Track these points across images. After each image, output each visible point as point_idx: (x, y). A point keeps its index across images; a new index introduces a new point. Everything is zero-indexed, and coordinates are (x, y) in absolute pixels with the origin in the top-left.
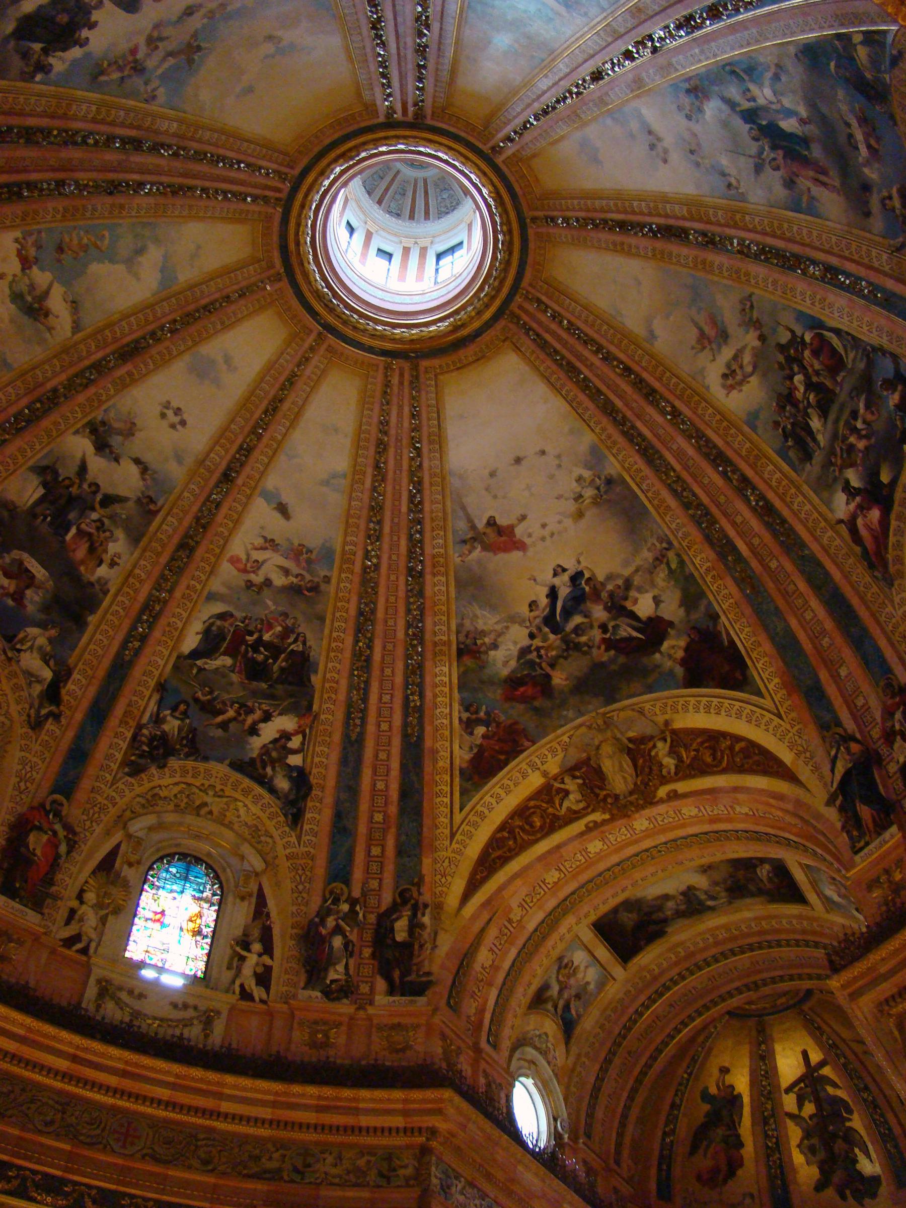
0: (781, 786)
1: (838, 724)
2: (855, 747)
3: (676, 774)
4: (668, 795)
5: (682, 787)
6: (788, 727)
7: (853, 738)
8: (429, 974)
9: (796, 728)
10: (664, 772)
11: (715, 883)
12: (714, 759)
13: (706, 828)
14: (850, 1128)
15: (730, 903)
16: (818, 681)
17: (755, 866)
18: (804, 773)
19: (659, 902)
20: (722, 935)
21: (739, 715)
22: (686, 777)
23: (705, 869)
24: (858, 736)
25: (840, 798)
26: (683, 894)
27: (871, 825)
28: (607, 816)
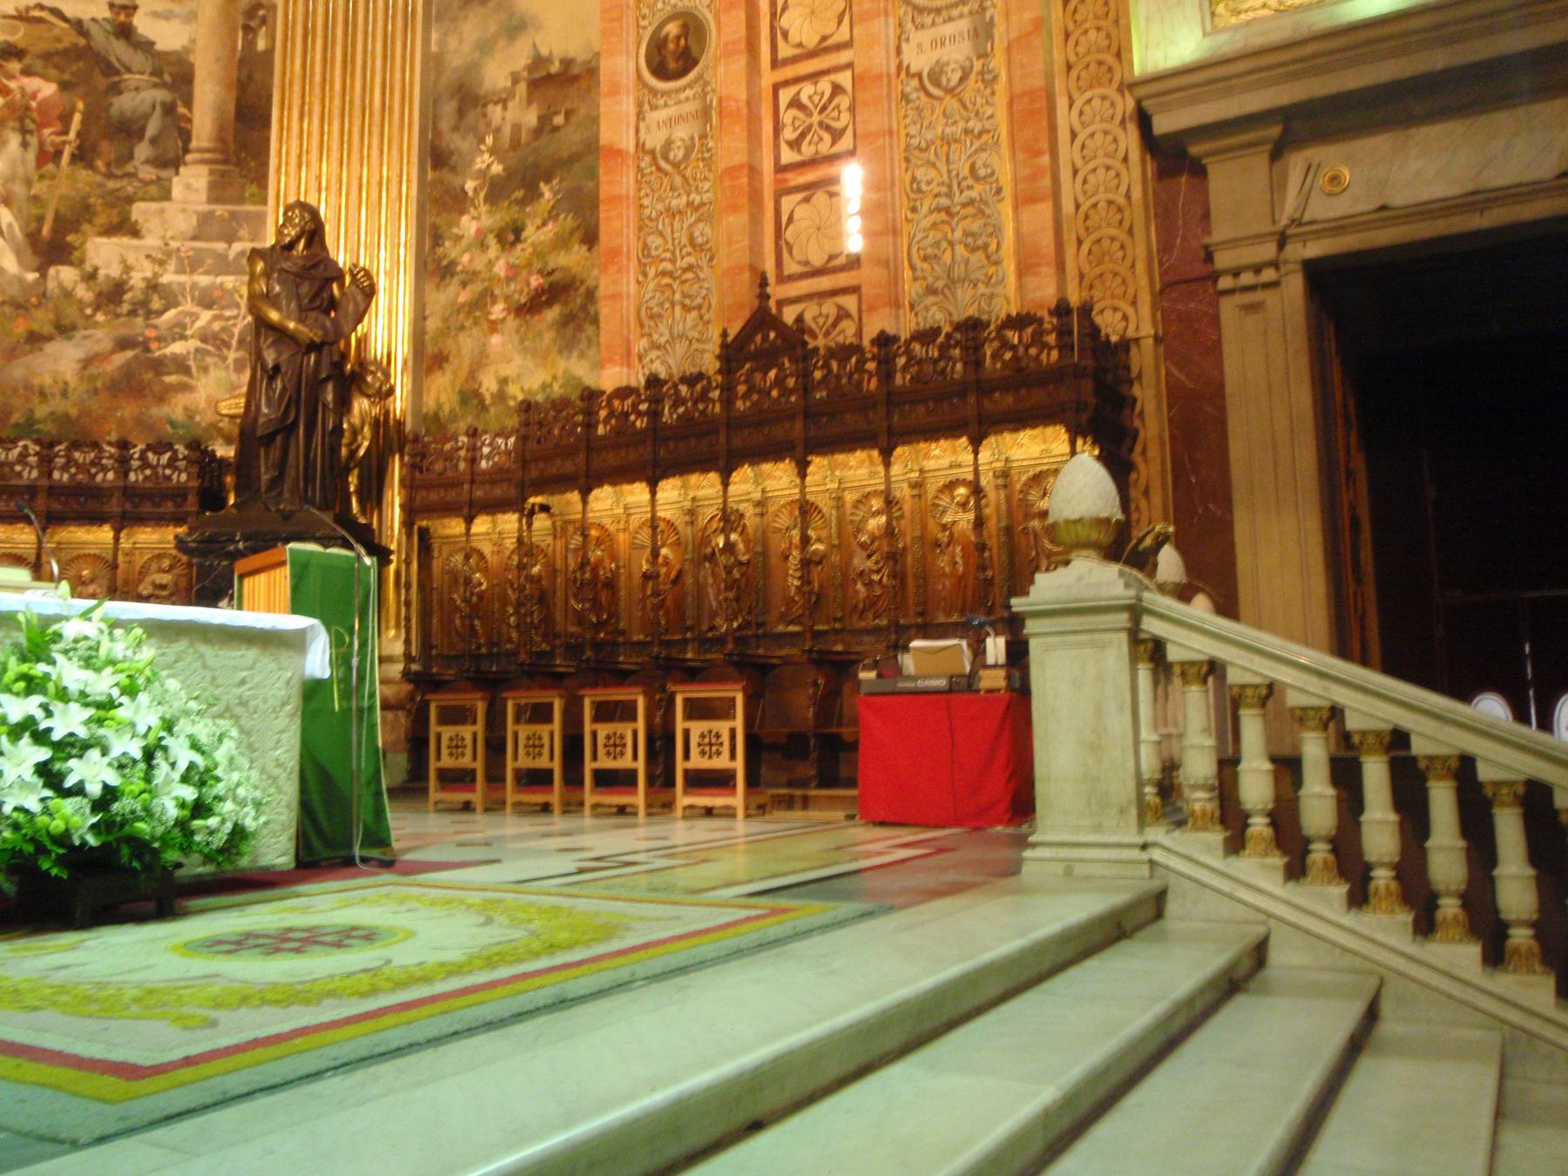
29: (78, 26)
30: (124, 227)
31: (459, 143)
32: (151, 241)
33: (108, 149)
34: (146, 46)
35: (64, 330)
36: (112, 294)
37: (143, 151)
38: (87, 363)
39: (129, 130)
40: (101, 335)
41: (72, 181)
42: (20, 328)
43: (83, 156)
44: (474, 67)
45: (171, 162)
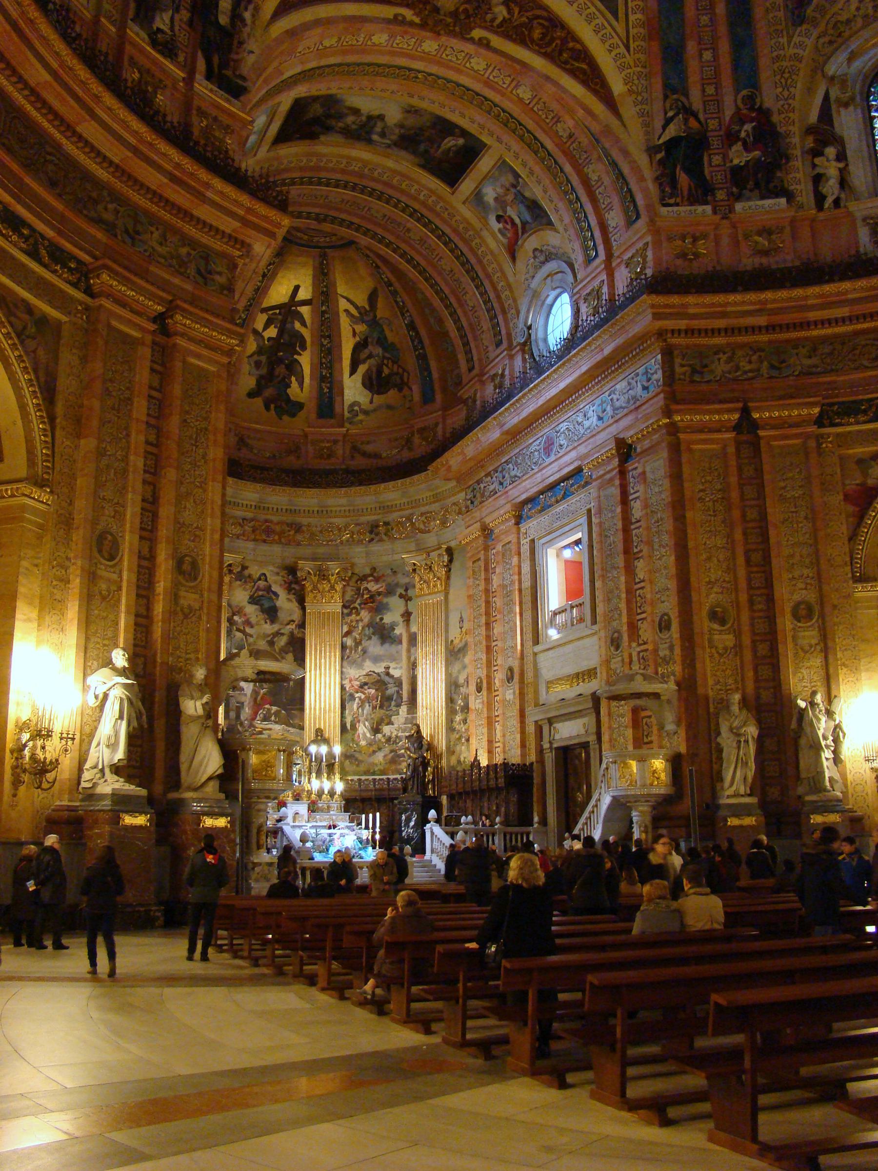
0: (599, 108)
1: (687, 96)
2: (693, 123)
3: (500, 25)
4: (480, 39)
5: (496, 41)
6: (632, 64)
7: (695, 115)
8: (244, 79)
9: (639, 69)
10: (489, 17)
11: (401, 126)
12: (541, 39)
13: (477, 87)
14: (296, 360)
15: (389, 146)
16: (683, 47)
17: (452, 134)
18: (629, 111)
19: (346, 111)
20: (355, 167)
21: (590, 19)
22: (507, 36)
23: (411, 111)
24: (701, 116)
25: (663, 153)
26: (370, 118)
27: (685, 193)
28: (417, 20)
29: (378, 674)
30: (390, 723)
31: (455, 697)
32: (396, 726)
33: (386, 704)
34: (392, 677)
35: (380, 749)
36: (389, 740)
37: (393, 703)
38: (385, 756)
39: (389, 699)
40: (387, 749)
41: (380, 713)
42: (371, 750)
43: (381, 707)
44: (457, 677)
45: (398, 705)
